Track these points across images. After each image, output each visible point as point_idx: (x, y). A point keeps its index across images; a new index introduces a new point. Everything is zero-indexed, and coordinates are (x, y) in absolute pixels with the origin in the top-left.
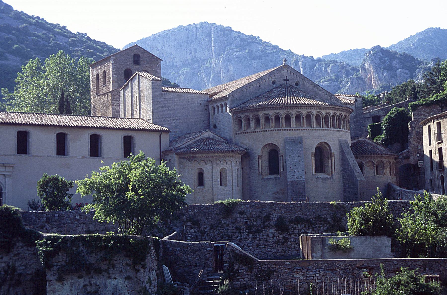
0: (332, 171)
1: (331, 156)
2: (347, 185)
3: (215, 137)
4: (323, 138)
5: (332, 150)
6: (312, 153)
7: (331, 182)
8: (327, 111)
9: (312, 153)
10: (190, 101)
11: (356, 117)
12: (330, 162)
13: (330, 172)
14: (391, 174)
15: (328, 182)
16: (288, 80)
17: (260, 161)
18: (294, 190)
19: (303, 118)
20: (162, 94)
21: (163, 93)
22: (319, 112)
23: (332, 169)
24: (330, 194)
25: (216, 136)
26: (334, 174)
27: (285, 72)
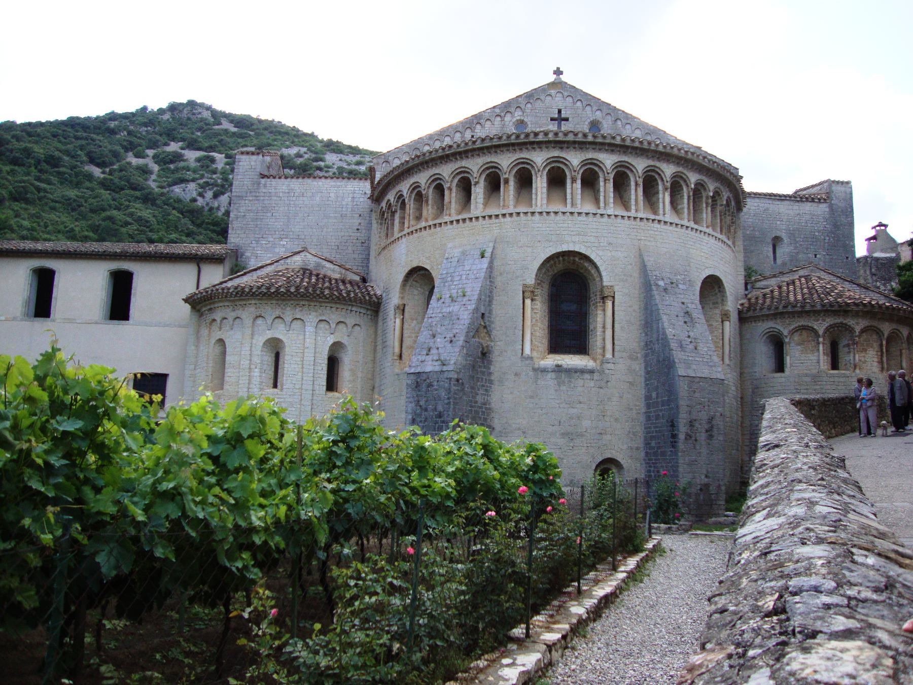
0: (604, 348)
1: (604, 298)
2: (654, 395)
3: (323, 267)
4: (567, 238)
5: (605, 279)
6: (525, 286)
7: (592, 384)
8: (590, 155)
9: (525, 286)
10: (332, 195)
11: (832, 232)
12: (600, 319)
13: (599, 351)
14: (882, 369)
15: (580, 382)
16: (567, 120)
17: (398, 321)
18: (422, 403)
19: (507, 181)
20: (259, 184)
21: (263, 181)
22: (557, 160)
23: (604, 339)
24: (586, 423)
25: (328, 265)
26: (609, 355)
27: (558, 102)
